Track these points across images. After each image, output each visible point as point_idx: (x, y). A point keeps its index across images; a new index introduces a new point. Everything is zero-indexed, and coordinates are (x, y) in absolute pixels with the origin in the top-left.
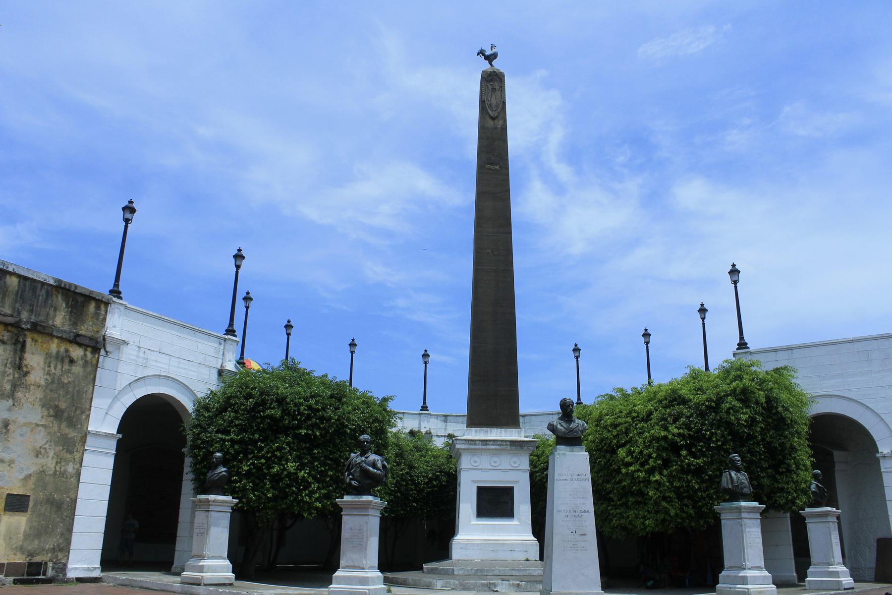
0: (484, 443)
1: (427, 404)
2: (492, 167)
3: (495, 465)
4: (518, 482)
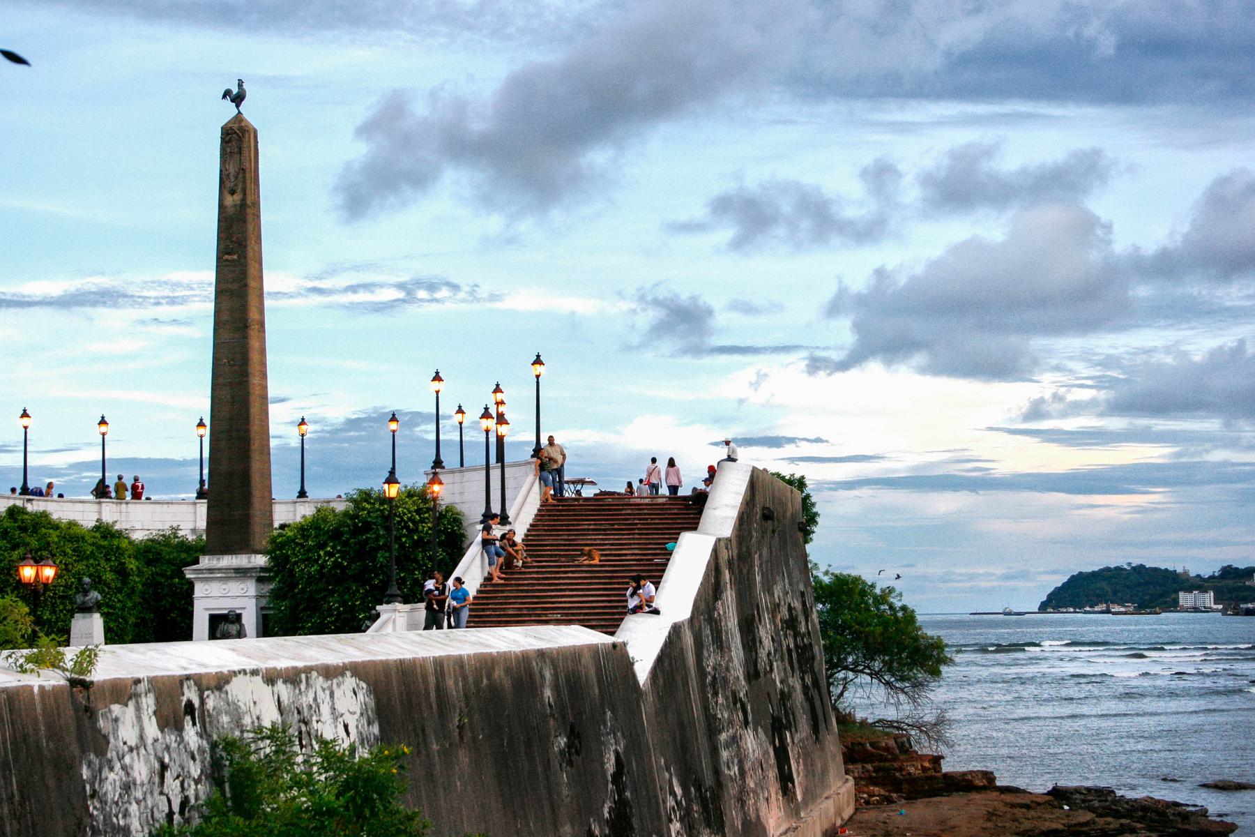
1: (306, 488)
2: (229, 257)
4: (244, 608)
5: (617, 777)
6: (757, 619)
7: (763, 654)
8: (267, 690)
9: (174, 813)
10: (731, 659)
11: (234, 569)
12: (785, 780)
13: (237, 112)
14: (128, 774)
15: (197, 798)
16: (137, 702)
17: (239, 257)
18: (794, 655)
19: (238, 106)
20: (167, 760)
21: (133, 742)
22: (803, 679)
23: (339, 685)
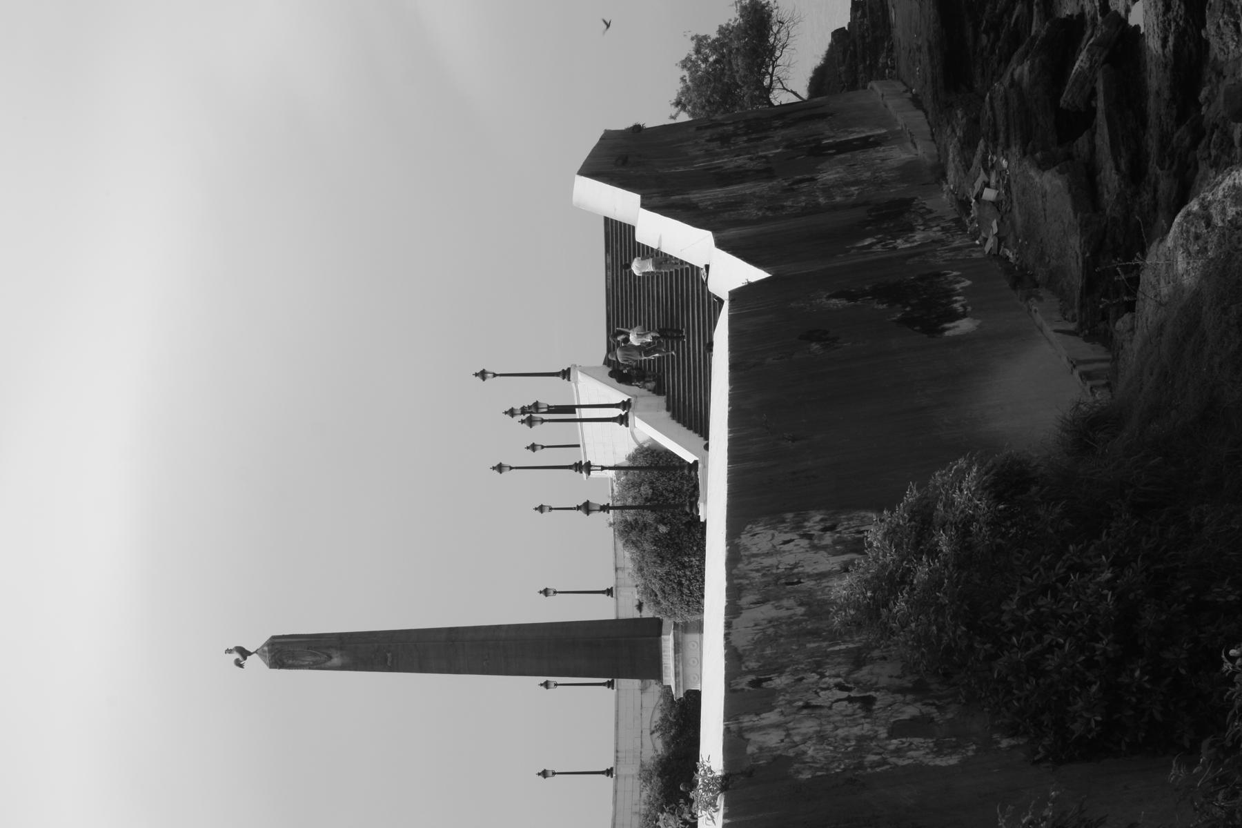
2: (389, 660)
3: (696, 661)
5: (850, 297)
6: (718, 170)
7: (751, 165)
8: (746, 615)
9: (849, 696)
10: (753, 194)
11: (675, 653)
12: (867, 144)
13: (255, 655)
14: (810, 738)
15: (838, 676)
16: (746, 731)
17: (389, 652)
18: (753, 136)
19: (250, 654)
20: (801, 703)
21: (781, 734)
22: (776, 128)
23: (747, 549)
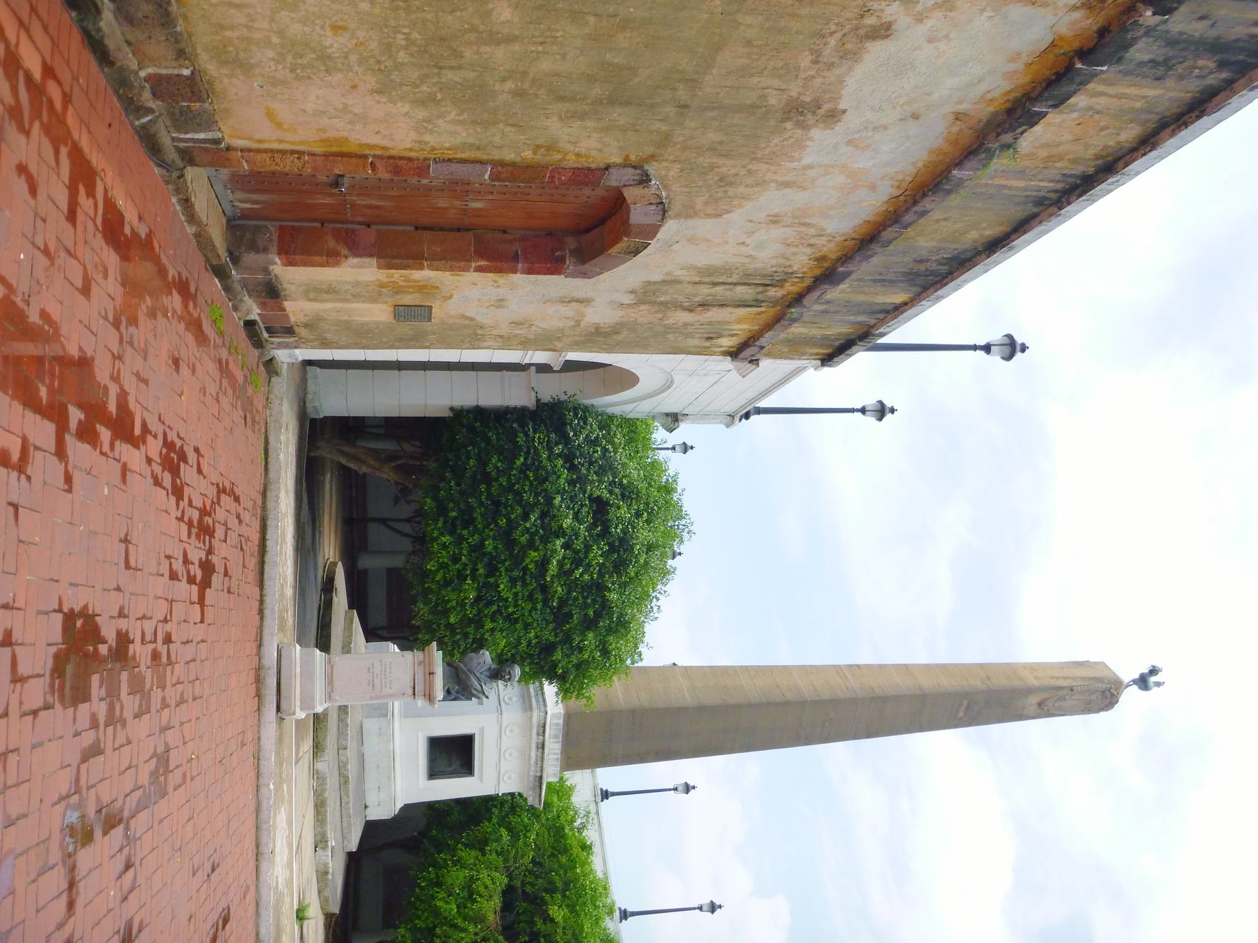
0: (540, 746)
2: (963, 708)
3: (507, 754)
4: (481, 780)
19: (1135, 682)
